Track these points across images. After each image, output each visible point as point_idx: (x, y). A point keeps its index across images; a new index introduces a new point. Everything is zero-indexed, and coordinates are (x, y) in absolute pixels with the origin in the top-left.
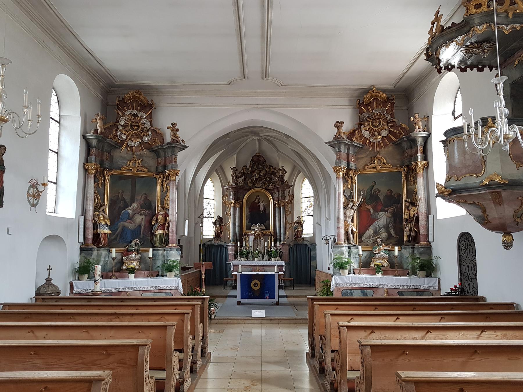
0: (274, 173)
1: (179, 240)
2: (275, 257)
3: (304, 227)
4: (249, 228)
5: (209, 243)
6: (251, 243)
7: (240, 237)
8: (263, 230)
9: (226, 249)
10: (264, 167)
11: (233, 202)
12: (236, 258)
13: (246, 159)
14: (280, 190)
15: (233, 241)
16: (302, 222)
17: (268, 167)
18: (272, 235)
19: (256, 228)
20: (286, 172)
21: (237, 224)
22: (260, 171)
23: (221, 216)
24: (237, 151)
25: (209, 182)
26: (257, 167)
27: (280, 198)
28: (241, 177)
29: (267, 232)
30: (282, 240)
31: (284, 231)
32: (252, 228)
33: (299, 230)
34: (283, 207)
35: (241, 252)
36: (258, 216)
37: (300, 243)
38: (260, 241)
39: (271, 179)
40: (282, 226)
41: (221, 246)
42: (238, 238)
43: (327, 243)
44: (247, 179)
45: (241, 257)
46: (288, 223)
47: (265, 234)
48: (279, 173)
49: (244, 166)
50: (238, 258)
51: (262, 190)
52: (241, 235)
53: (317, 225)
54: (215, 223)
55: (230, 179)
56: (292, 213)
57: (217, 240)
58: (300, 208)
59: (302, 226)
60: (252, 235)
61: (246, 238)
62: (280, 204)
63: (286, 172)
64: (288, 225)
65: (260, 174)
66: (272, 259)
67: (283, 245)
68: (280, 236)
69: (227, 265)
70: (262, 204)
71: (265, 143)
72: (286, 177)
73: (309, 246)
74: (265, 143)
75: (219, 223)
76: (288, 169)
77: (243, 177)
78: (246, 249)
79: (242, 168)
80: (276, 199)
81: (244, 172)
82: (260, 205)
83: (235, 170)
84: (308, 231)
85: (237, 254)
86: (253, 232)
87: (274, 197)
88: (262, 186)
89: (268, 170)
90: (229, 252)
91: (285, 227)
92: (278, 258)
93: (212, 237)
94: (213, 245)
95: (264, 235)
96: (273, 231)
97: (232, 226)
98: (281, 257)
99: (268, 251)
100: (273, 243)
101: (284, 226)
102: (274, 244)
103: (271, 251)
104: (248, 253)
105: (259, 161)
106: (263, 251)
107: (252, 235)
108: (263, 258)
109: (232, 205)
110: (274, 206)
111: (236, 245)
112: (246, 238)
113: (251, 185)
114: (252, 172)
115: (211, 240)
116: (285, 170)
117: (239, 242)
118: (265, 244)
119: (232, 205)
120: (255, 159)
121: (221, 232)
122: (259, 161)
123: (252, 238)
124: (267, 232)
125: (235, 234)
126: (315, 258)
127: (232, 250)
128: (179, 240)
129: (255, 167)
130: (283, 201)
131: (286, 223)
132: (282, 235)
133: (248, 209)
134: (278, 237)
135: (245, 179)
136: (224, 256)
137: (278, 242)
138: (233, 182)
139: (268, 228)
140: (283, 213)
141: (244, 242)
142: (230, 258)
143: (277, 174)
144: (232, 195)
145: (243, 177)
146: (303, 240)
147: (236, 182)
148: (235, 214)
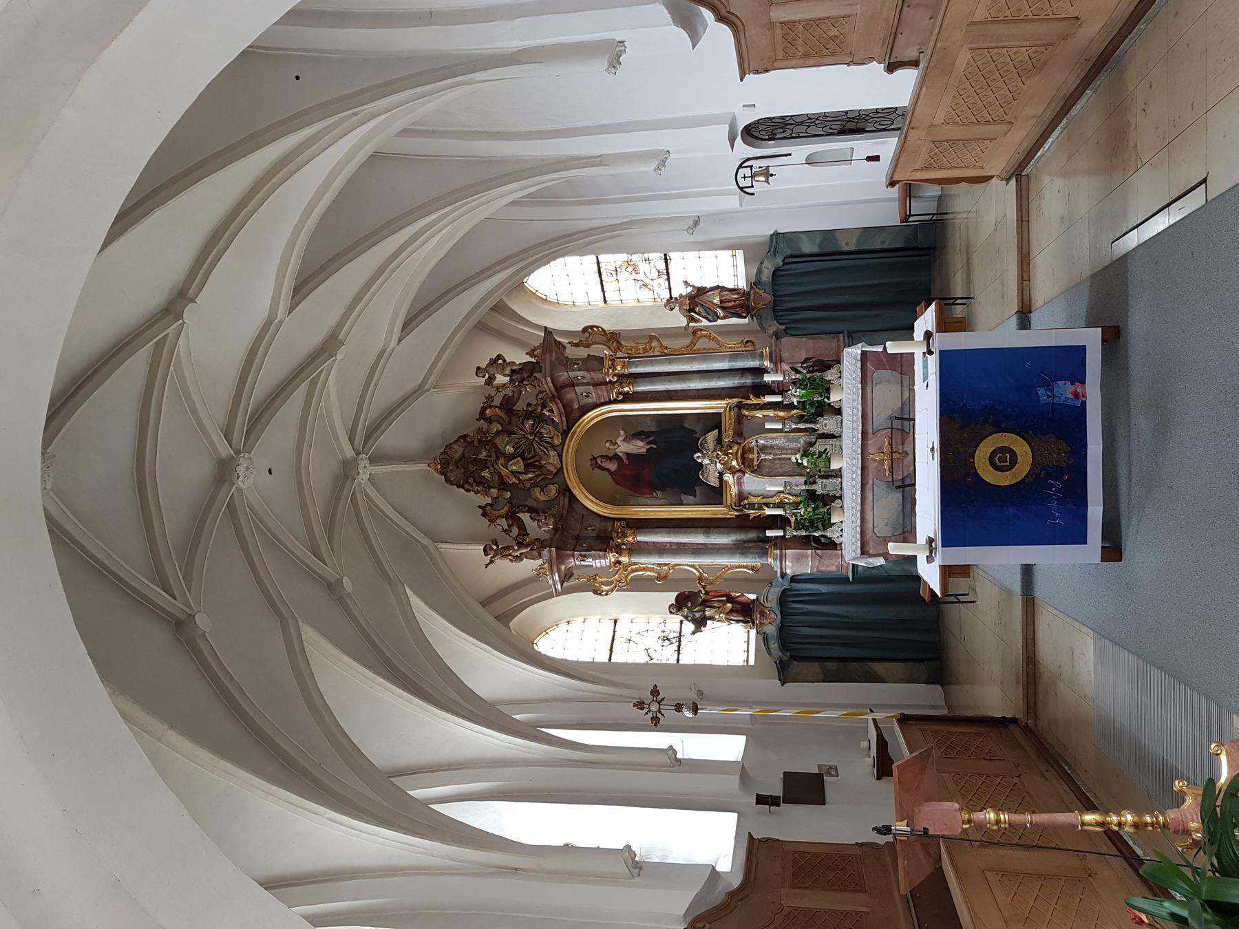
0: (508, 405)
2: (826, 389)
4: (715, 494)
5: (774, 645)
6: (772, 486)
7: (752, 527)
8: (719, 441)
9: (794, 579)
10: (485, 441)
11: (612, 557)
12: (832, 545)
13: (459, 508)
14: (563, 376)
15: (764, 553)
16: (690, 289)
18: (740, 406)
19: (712, 466)
21: (699, 539)
22: (500, 453)
23: (671, 597)
26: (484, 465)
27: (597, 376)
28: (522, 527)
29: (728, 422)
31: (722, 358)
32: (714, 482)
33: (717, 300)
34: (630, 364)
35: (812, 524)
37: (768, 297)
38: (763, 449)
41: (784, 598)
42: (752, 535)
43: (767, 174)
44: (531, 503)
45: (827, 524)
46: (693, 343)
47: (734, 432)
49: (484, 515)
50: (832, 533)
51: (571, 444)
52: (741, 523)
53: (699, 233)
54: (700, 623)
55: (529, 566)
57: (762, 614)
58: (640, 309)
59: (701, 291)
60: (739, 483)
61: (752, 506)
63: (499, 357)
66: (834, 398)
67: (777, 359)
69: (861, 577)
70: (623, 447)
72: (519, 357)
76: (489, 350)
77: (525, 517)
78: (796, 505)
79: (492, 521)
80: (603, 393)
81: (507, 517)
83: (495, 550)
84: (726, 270)
85: (817, 540)
86: (728, 477)
87: (593, 399)
88: (554, 447)
89: (496, 427)
90: (807, 568)
91: (705, 355)
92: (830, 375)
93: (753, 632)
94: (782, 629)
95: (739, 434)
97: (706, 561)
98: (826, 366)
99: (801, 419)
100: (769, 399)
101: (704, 359)
102: (774, 393)
103: (803, 405)
104: (812, 496)
105: (463, 461)
106: (803, 439)
107: (739, 483)
108: (832, 436)
109: (625, 559)
110: (627, 398)
111: (782, 543)
112: (752, 506)
113: (553, 490)
114: (503, 485)
115: (764, 638)
116: (493, 362)
117: (769, 533)
118: (775, 431)
119: (625, 559)
120: (455, 474)
121: (730, 599)
122: (463, 461)
123: (752, 483)
124: (728, 422)
125: (739, 548)
126: (829, 235)
127: (798, 559)
129: (486, 474)
130: (607, 363)
131: (691, 352)
132: (740, 364)
133: (642, 500)
134: (748, 380)
135: (532, 511)
136: (823, 588)
137: (768, 378)
138: (540, 556)
139: (713, 421)
141: (769, 512)
142: (830, 564)
143: (509, 392)
144: (589, 562)
145: (525, 517)
146: (755, 284)
147: (538, 546)
148: (661, 549)
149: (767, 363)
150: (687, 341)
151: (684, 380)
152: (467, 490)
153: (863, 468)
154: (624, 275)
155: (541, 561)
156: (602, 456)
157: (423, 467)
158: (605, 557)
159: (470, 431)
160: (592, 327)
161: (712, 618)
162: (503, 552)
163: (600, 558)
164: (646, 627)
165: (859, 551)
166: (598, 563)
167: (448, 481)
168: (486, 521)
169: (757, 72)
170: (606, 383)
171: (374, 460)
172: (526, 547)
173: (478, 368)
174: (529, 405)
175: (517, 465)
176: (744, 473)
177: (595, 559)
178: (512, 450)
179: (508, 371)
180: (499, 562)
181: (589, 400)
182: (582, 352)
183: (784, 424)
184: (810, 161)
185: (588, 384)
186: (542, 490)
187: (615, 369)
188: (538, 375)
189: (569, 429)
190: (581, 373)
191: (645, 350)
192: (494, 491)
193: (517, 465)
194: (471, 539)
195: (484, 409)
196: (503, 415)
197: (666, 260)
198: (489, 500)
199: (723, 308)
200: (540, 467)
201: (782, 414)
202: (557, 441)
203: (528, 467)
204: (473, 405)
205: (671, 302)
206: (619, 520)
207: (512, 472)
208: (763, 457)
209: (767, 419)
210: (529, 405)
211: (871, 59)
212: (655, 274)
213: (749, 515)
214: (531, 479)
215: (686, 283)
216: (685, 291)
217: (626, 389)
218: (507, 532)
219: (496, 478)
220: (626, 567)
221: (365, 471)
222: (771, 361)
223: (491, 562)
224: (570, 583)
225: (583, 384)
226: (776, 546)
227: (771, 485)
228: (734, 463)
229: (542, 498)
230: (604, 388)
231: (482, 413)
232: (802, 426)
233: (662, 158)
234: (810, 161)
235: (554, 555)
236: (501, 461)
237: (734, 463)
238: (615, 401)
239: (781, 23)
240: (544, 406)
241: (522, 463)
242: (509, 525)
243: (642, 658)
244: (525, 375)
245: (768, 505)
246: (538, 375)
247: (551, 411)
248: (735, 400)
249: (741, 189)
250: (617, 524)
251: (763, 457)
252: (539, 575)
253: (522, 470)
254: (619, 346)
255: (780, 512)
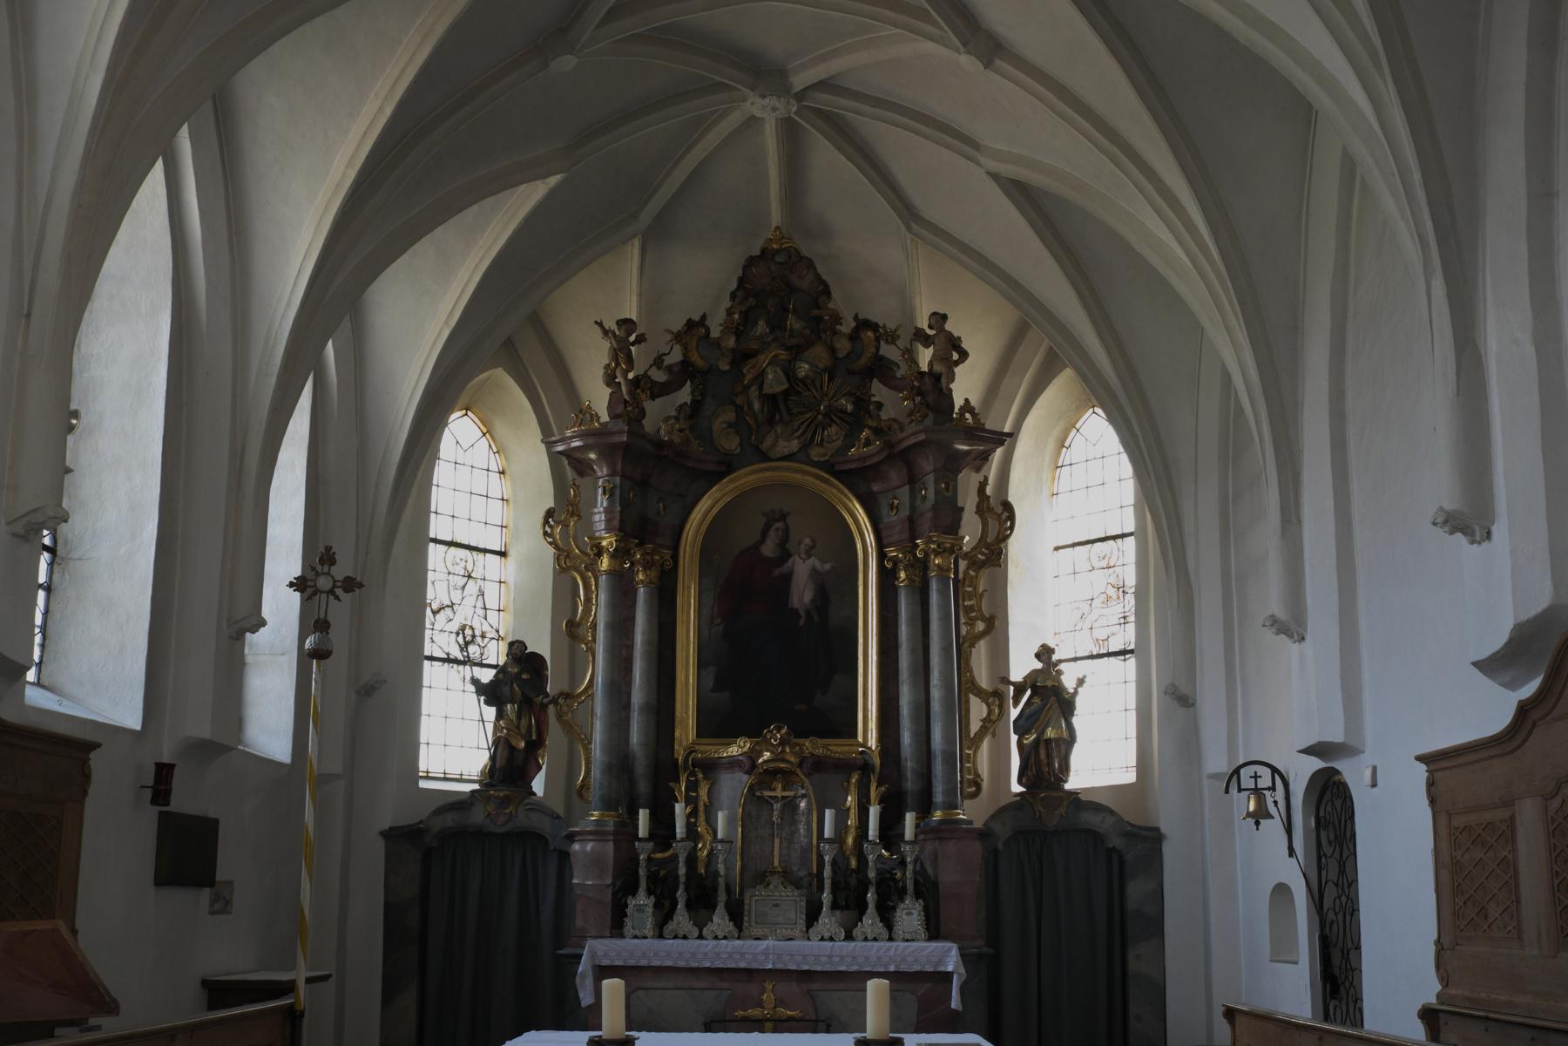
0: (880, 369)
1: (164, 772)
3: (1075, 721)
5: (450, 820)
9: (564, 856)
11: (608, 541)
13: (703, 280)
14: (927, 464)
17: (847, 326)
18: (865, 768)
20: (964, 355)
21: (637, 696)
22: (797, 351)
23: (540, 644)
24: (646, 217)
25: (461, 431)
26: (777, 325)
29: (837, 748)
30: (938, 797)
33: (1050, 733)
34: (944, 581)
36: (778, 663)
38: (790, 805)
39: (864, 404)
40: (936, 707)
41: (530, 838)
42: (643, 787)
43: (1260, 815)
46: (980, 693)
48: (913, 361)
51: (808, 478)
52: (664, 768)
53: (1172, 705)
54: (490, 693)
55: (598, 398)
56: (995, 625)
57: (505, 802)
59: (1066, 705)
61: (693, 786)
62: (924, 565)
64: (978, 710)
65: (789, 373)
68: (926, 776)
70: (802, 569)
71: (825, 157)
72: (966, 386)
73: (1115, 842)
74: (825, 157)
75: (518, 687)
77: (685, 395)
78: (692, 860)
79: (678, 337)
81: (685, 363)
82: (787, 578)
83: (623, 337)
87: (889, 517)
88: (805, 447)
89: (843, 346)
95: (818, 766)
96: (872, 742)
100: (874, 811)
107: (733, 763)
109: (605, 563)
112: (693, 786)
113: (731, 444)
114: (742, 357)
116: (955, 344)
117: (643, 815)
119: (605, 563)
121: (535, 745)
122: (783, 288)
123: (733, 786)
124: (837, 748)
125: (620, 763)
128: (164, 772)
129: (761, 327)
130: (948, 541)
132: (938, 768)
134: (911, 784)
135: (694, 410)
137: (910, 818)
138: (614, 416)
140: (945, 617)
144: (602, 502)
145: (685, 395)
147: (628, 407)
148: (621, 627)
149: (938, 815)
150: (984, 682)
151: (914, 673)
152: (733, 296)
153: (749, 974)
154: (1101, 581)
155: (605, 418)
156: (787, 530)
157: (776, 218)
158: (608, 529)
159: (838, 301)
160: (1012, 517)
161: (500, 715)
162: (621, 353)
163: (608, 521)
164: (492, 603)
165: (606, 962)
166: (599, 518)
167: (751, 262)
168: (678, 325)
169: (1431, 784)
170: (913, 538)
171: (790, 133)
172: (630, 393)
173: (944, 317)
174: (880, 406)
175: (775, 381)
176: (748, 772)
177: (608, 511)
178: (802, 374)
179: (938, 368)
180: (605, 346)
181: (885, 511)
182: (969, 502)
183: (829, 841)
184: (1281, 891)
185: (913, 507)
186: (730, 425)
187: (937, 554)
188: (929, 421)
189: (838, 475)
190: (931, 495)
191: (969, 609)
192: (731, 342)
193: (775, 381)
194: (652, 298)
195: (874, 326)
196: (863, 361)
197: (1123, 653)
198: (715, 333)
199: (1037, 743)
200: (771, 422)
201: (850, 840)
202: (815, 453)
203: (772, 399)
204: (882, 312)
205: (1045, 653)
206: (675, 557)
207: (762, 374)
208: (777, 806)
209: (841, 816)
210: (880, 406)
211: (1445, 979)
212: (1101, 634)
213: (678, 781)
214: (750, 405)
215: (1081, 682)
216: (1068, 682)
217: (902, 575)
218: (658, 362)
219: (755, 346)
220: (592, 567)
221: (765, 109)
222: (942, 822)
223: (606, 332)
224: (568, 467)
225: (913, 495)
226: (621, 824)
227: (730, 821)
228: (767, 755)
229: (717, 426)
230: (906, 535)
231: (864, 324)
232: (827, 872)
233: (1292, 627)
234: (1281, 891)
235: (616, 439)
236: (783, 355)
237: (767, 755)
238: (882, 556)
239: (1512, 818)
240: (878, 431)
241: (779, 389)
242: (670, 368)
243: (436, 592)
244: (930, 398)
245: (694, 813)
246: (929, 421)
247: (868, 443)
248: (877, 761)
249: (1237, 772)
250: (667, 553)
251: (777, 806)
252: (585, 414)
253: (767, 390)
254: (975, 565)
255: (680, 830)
